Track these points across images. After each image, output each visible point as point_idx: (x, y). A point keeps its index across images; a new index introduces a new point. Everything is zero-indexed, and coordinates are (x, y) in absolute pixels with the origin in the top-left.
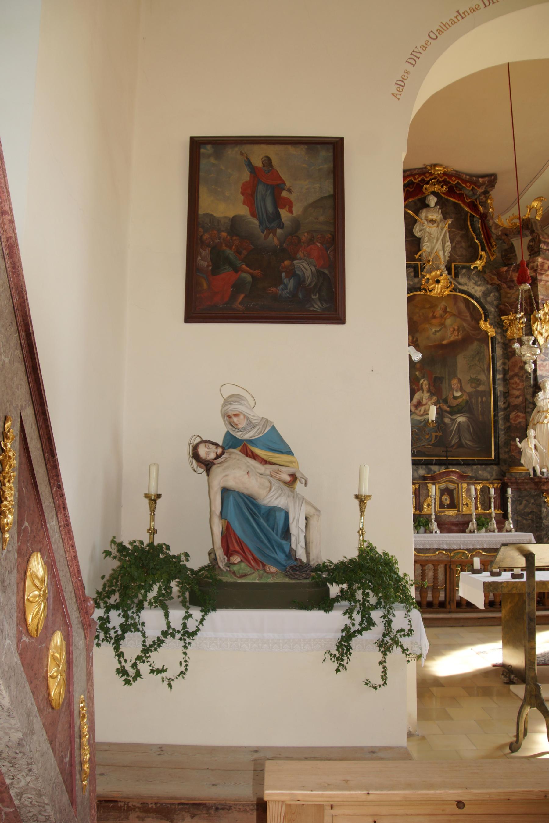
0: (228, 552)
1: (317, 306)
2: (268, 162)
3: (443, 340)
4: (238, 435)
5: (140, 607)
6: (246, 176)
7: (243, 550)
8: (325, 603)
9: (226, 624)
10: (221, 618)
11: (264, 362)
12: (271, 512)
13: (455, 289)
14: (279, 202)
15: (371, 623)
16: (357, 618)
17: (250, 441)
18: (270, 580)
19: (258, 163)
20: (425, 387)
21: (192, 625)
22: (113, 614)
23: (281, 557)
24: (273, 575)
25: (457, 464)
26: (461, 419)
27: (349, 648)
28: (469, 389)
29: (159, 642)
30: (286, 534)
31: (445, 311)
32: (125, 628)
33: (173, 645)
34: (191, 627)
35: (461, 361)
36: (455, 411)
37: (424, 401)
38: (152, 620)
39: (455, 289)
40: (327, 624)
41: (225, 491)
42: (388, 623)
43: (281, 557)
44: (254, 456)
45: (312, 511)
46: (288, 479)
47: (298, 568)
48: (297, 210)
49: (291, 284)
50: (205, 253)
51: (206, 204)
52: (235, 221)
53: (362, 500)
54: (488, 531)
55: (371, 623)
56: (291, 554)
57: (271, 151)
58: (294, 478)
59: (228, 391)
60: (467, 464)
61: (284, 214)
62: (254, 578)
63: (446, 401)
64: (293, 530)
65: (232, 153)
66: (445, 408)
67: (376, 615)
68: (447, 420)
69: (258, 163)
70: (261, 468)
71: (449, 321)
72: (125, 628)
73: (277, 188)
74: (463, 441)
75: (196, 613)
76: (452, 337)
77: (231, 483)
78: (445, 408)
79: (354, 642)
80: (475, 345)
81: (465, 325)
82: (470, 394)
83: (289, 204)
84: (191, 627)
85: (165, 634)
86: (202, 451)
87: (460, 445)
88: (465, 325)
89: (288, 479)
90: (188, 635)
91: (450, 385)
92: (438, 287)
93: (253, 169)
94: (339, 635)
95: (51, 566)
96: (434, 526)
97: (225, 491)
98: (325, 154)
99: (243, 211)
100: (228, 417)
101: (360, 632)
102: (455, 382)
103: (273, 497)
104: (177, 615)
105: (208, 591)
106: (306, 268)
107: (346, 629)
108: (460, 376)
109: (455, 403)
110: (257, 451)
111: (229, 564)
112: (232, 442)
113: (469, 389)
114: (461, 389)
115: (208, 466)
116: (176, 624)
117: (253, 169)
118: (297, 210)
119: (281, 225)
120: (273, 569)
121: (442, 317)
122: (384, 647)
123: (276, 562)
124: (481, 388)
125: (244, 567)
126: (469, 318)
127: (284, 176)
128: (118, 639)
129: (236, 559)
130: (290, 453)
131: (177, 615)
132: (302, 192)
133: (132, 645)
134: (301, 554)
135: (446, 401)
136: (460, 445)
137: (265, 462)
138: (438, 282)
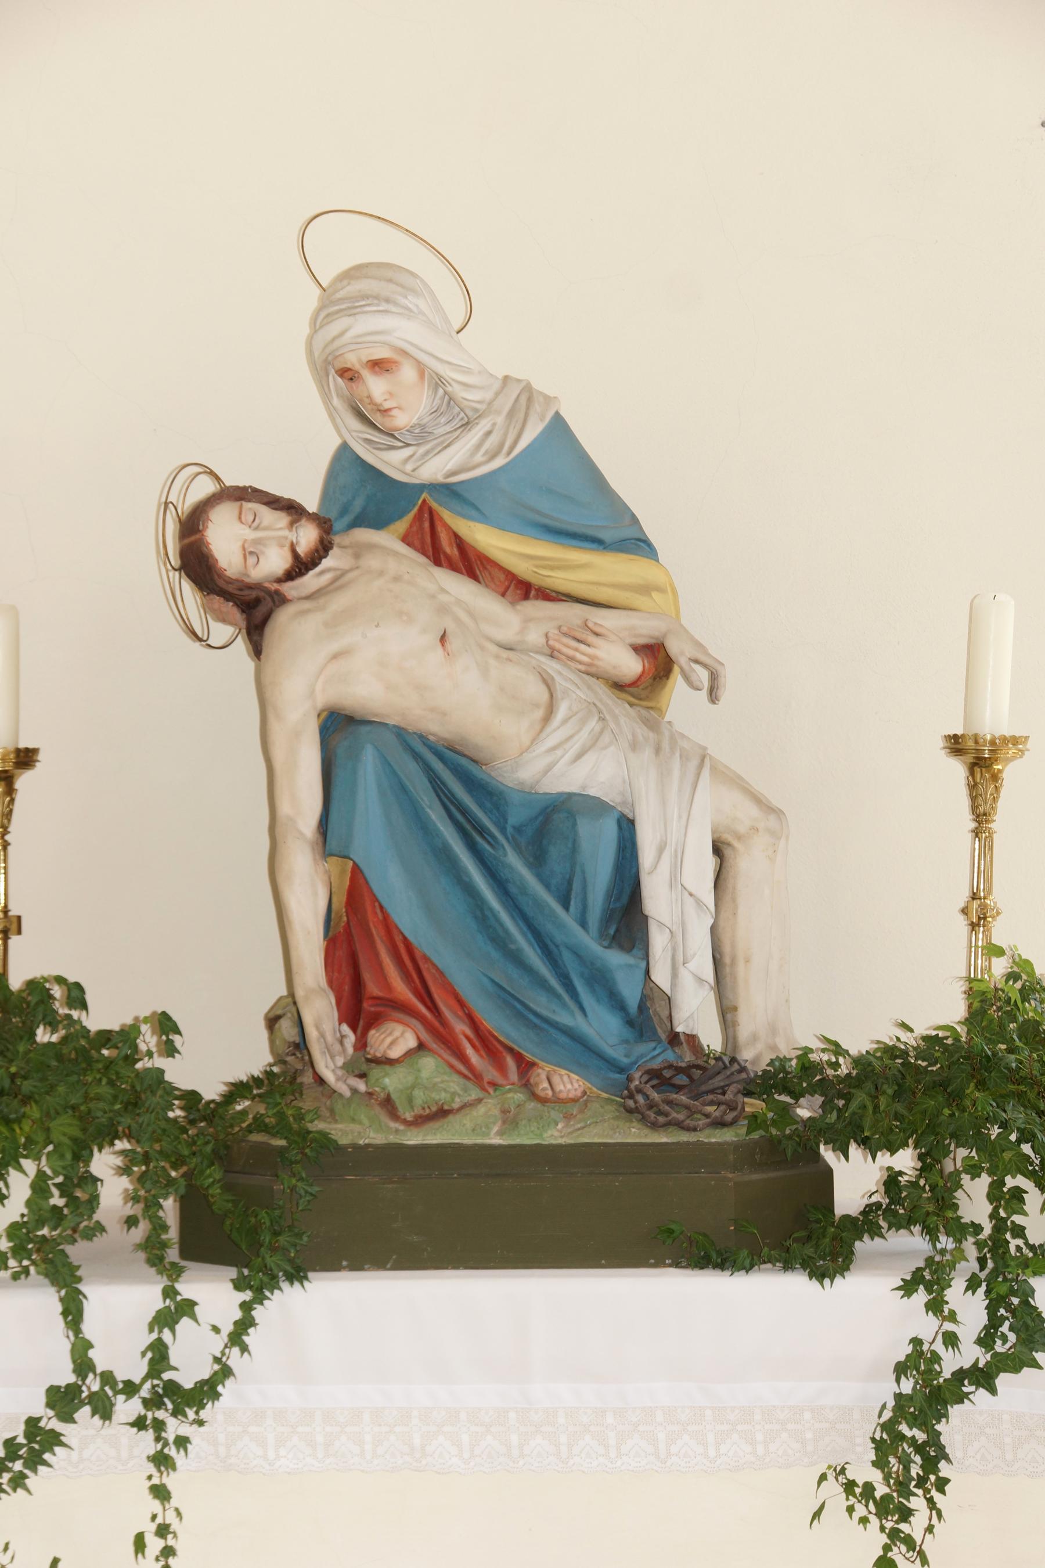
0: (359, 1010)
4: (394, 463)
7: (428, 998)
8: (814, 1240)
9: (352, 1341)
10: (330, 1313)
12: (552, 822)
16: (970, 1310)
17: (450, 491)
18: (556, 1134)
21: (191, 1357)
23: (603, 1027)
24: (568, 1110)
27: (933, 1454)
30: (627, 918)
34: (189, 1366)
41: (339, 727)
43: (603, 1027)
44: (470, 563)
45: (743, 813)
46: (631, 666)
47: (682, 1078)
53: (980, 759)
56: (648, 1016)
58: (658, 660)
59: (338, 249)
62: (481, 1125)
64: (658, 900)
75: (214, 1293)
77: (366, 691)
79: (957, 1427)
84: (189, 1366)
85: (63, 1400)
86: (226, 540)
89: (631, 666)
90: (176, 1398)
94: (885, 1390)
97: (339, 727)
100: (343, 377)
101: (983, 1377)
103: (557, 751)
104: (120, 1309)
105: (263, 1191)
107: (918, 1361)
110: (486, 538)
111: (365, 1063)
112: (365, 499)
115: (255, 609)
116: (120, 1353)
120: (569, 1084)
123: (583, 1052)
125: (434, 1077)
129: (397, 1038)
130: (638, 544)
131: (120, 1309)
134: (696, 1014)
137: (522, 589)
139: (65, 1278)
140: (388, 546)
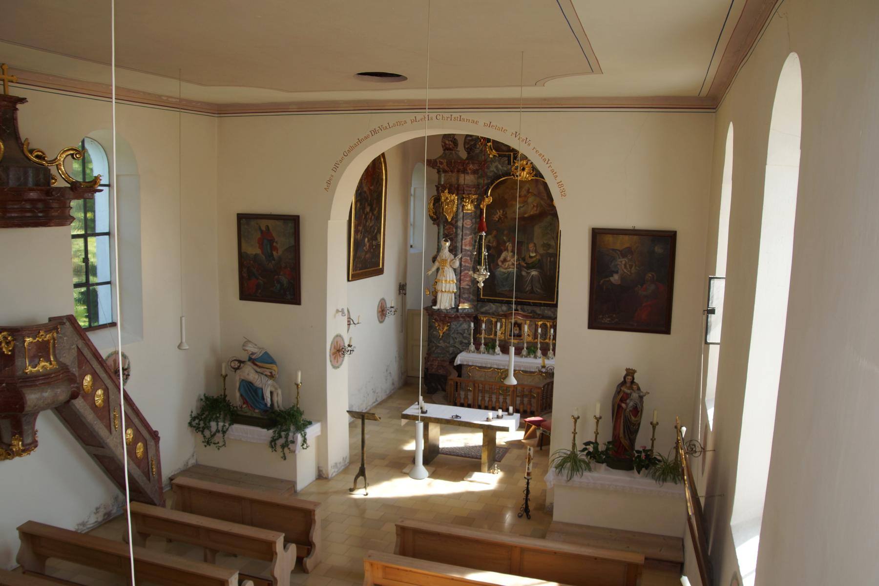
1: (289, 297)
2: (267, 227)
3: (525, 213)
5: (210, 421)
6: (259, 235)
9: (238, 430)
10: (237, 427)
11: (266, 321)
13: (536, 175)
14: (273, 248)
15: (280, 437)
18: (255, 415)
19: (264, 229)
20: (510, 248)
22: (202, 422)
24: (257, 413)
25: (529, 304)
26: (534, 273)
28: (541, 251)
29: (215, 434)
30: (263, 399)
31: (528, 192)
32: (204, 428)
33: (220, 435)
35: (537, 230)
36: (530, 267)
37: (509, 258)
38: (213, 424)
39: (536, 175)
40: (266, 434)
42: (287, 436)
43: (262, 406)
45: (273, 389)
48: (280, 252)
49: (278, 286)
50: (245, 270)
51: (245, 248)
52: (256, 256)
54: (535, 357)
55: (280, 437)
56: (266, 405)
57: (270, 223)
60: (535, 304)
61: (274, 253)
62: (249, 414)
63: (524, 259)
65: (253, 223)
66: (523, 264)
67: (283, 434)
68: (524, 273)
69: (264, 229)
70: (259, 370)
71: (530, 200)
72: (204, 428)
73: (271, 241)
74: (535, 289)
76: (532, 211)
78: (523, 264)
80: (549, 217)
81: (542, 203)
82: (542, 255)
83: (276, 249)
86: (233, 364)
87: (532, 291)
88: (542, 203)
90: (224, 432)
91: (528, 248)
92: (524, 174)
93: (262, 232)
94: (270, 439)
96: (498, 349)
98: (291, 224)
99: (258, 251)
102: (531, 246)
106: (284, 280)
107: (273, 437)
108: (535, 241)
109: (530, 261)
113: (541, 251)
114: (536, 251)
116: (220, 428)
117: (262, 232)
118: (280, 252)
119: (274, 259)
121: (525, 196)
122: (283, 447)
124: (551, 251)
126: (546, 198)
127: (274, 235)
128: (202, 432)
132: (282, 243)
133: (207, 433)
135: (524, 259)
136: (532, 291)
137: (260, 367)
138: (523, 169)
140: (249, 363)
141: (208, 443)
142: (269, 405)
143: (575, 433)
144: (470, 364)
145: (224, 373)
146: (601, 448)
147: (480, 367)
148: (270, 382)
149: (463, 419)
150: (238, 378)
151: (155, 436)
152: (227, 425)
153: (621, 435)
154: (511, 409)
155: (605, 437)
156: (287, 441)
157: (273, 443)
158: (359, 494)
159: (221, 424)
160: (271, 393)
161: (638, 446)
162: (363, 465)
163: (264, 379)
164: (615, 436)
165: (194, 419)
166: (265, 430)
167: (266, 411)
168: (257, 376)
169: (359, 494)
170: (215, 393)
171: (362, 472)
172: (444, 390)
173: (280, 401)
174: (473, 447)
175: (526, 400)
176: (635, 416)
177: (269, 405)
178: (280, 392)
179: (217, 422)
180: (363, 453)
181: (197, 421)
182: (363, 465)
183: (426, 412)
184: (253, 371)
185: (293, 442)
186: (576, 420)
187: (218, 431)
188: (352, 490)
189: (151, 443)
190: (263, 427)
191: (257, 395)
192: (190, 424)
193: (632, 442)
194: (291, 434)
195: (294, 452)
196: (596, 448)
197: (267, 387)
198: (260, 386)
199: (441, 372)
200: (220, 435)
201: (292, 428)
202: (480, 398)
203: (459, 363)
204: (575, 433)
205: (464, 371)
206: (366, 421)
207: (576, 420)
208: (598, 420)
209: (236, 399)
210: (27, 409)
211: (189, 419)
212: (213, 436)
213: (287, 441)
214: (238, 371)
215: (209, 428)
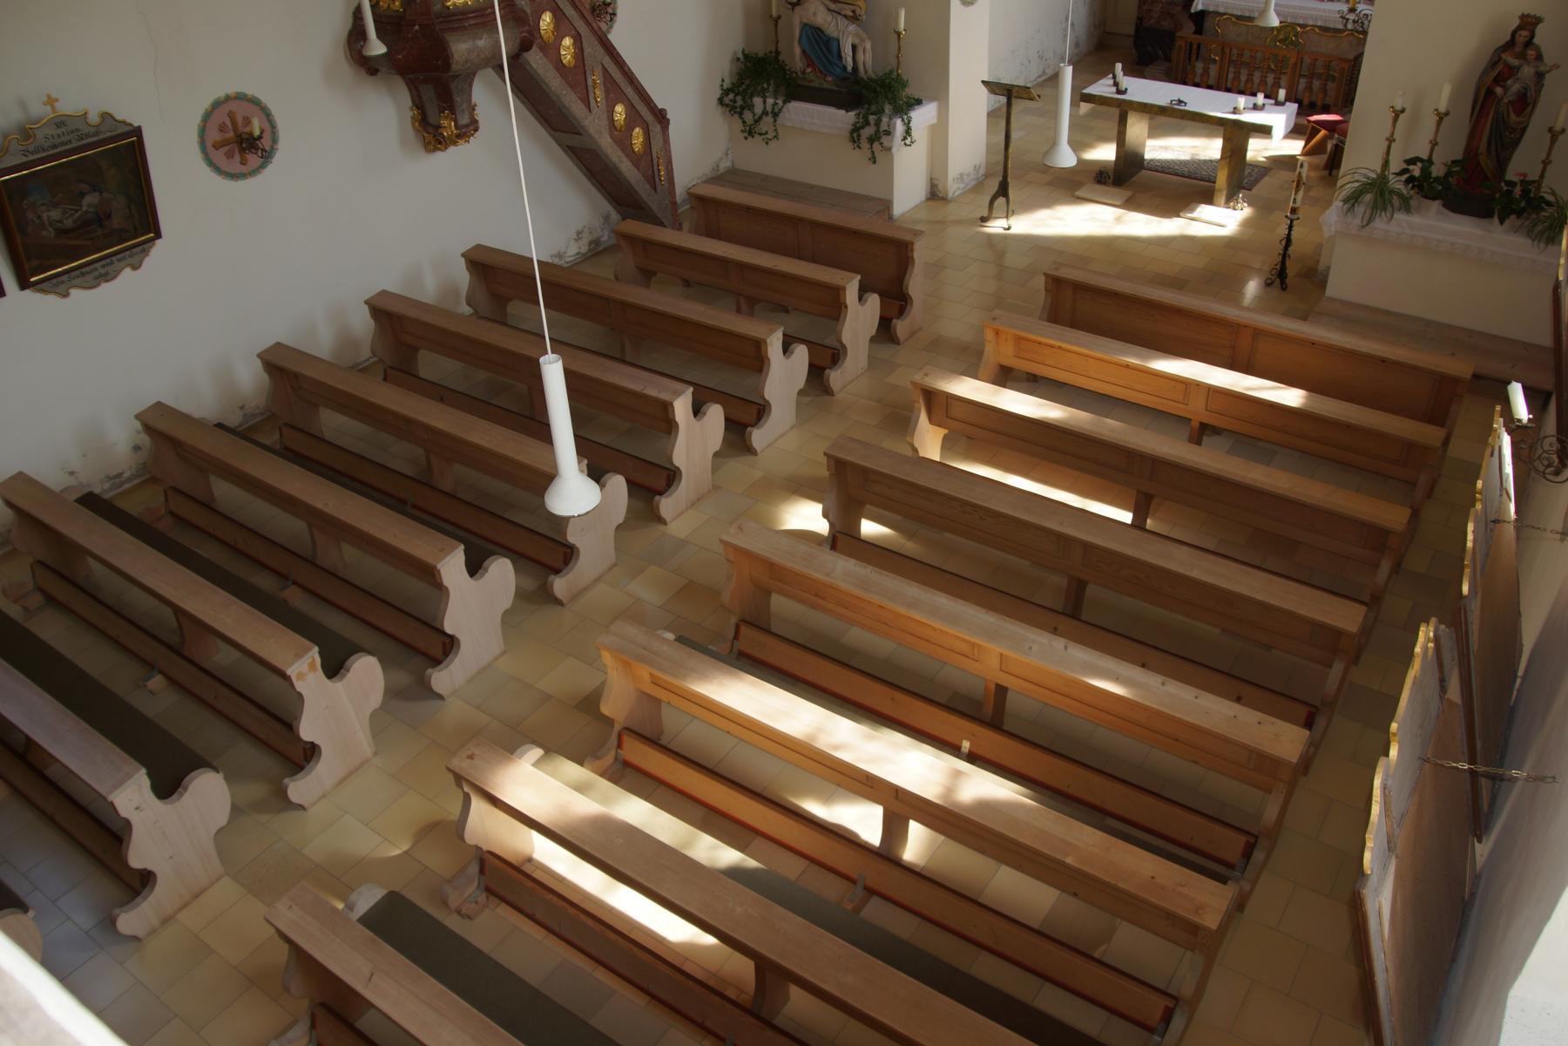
5: (752, 96)
9: (799, 113)
10: (795, 105)
15: (867, 123)
18: (825, 86)
22: (739, 98)
24: (828, 83)
29: (760, 118)
30: (840, 57)
32: (742, 108)
33: (769, 119)
38: (758, 101)
40: (843, 119)
43: (839, 71)
45: (857, 41)
55: (867, 123)
56: (845, 68)
62: (816, 84)
67: (872, 118)
72: (742, 108)
90: (775, 115)
94: (850, 127)
95: (631, 108)
104: (770, 101)
116: (769, 108)
122: (871, 140)
125: (812, 76)
128: (741, 114)
133: (748, 116)
139: (764, 97)
141: (750, 132)
142: (850, 68)
143: (1391, 140)
144: (1221, 10)
145: (774, 14)
146: (1437, 171)
147: (1238, 17)
148: (852, 28)
149: (1191, 107)
150: (797, 22)
151: (661, 117)
152: (780, 102)
153: (1483, 148)
154: (1282, 93)
155: (1451, 150)
156: (877, 131)
157: (855, 135)
158: (996, 226)
159: (770, 101)
160: (854, 47)
161: (1511, 174)
162: (1005, 177)
163: (842, 22)
164: (1470, 151)
165: (726, 92)
166: (843, 112)
167: (845, 79)
168: (829, 18)
169: (996, 226)
170: (760, 49)
171: (1003, 190)
172: (1168, 59)
173: (867, 61)
174: (1205, 162)
175: (1316, 84)
176: (1518, 114)
177: (850, 68)
178: (868, 45)
179: (764, 97)
180: (1006, 157)
181: (731, 96)
182: (1005, 177)
183: (1124, 92)
184: (822, 8)
185: (888, 133)
186: (1397, 114)
187: (765, 113)
188: (984, 220)
189: (656, 129)
190: (839, 107)
191: (830, 51)
192: (721, 101)
193: (1502, 165)
194: (885, 119)
195: (890, 149)
196: (1426, 172)
197: (847, 36)
198: (835, 35)
199: (1166, 24)
200: (769, 119)
201: (888, 108)
202: (1231, 76)
203: (1200, 7)
204: (1391, 140)
205: (1207, 24)
206: (1014, 101)
207: (1397, 114)
208: (1441, 117)
209: (794, 57)
210: (455, 67)
211: (718, 93)
212: (758, 121)
213: (877, 131)
214: (798, 9)
215: (751, 107)
